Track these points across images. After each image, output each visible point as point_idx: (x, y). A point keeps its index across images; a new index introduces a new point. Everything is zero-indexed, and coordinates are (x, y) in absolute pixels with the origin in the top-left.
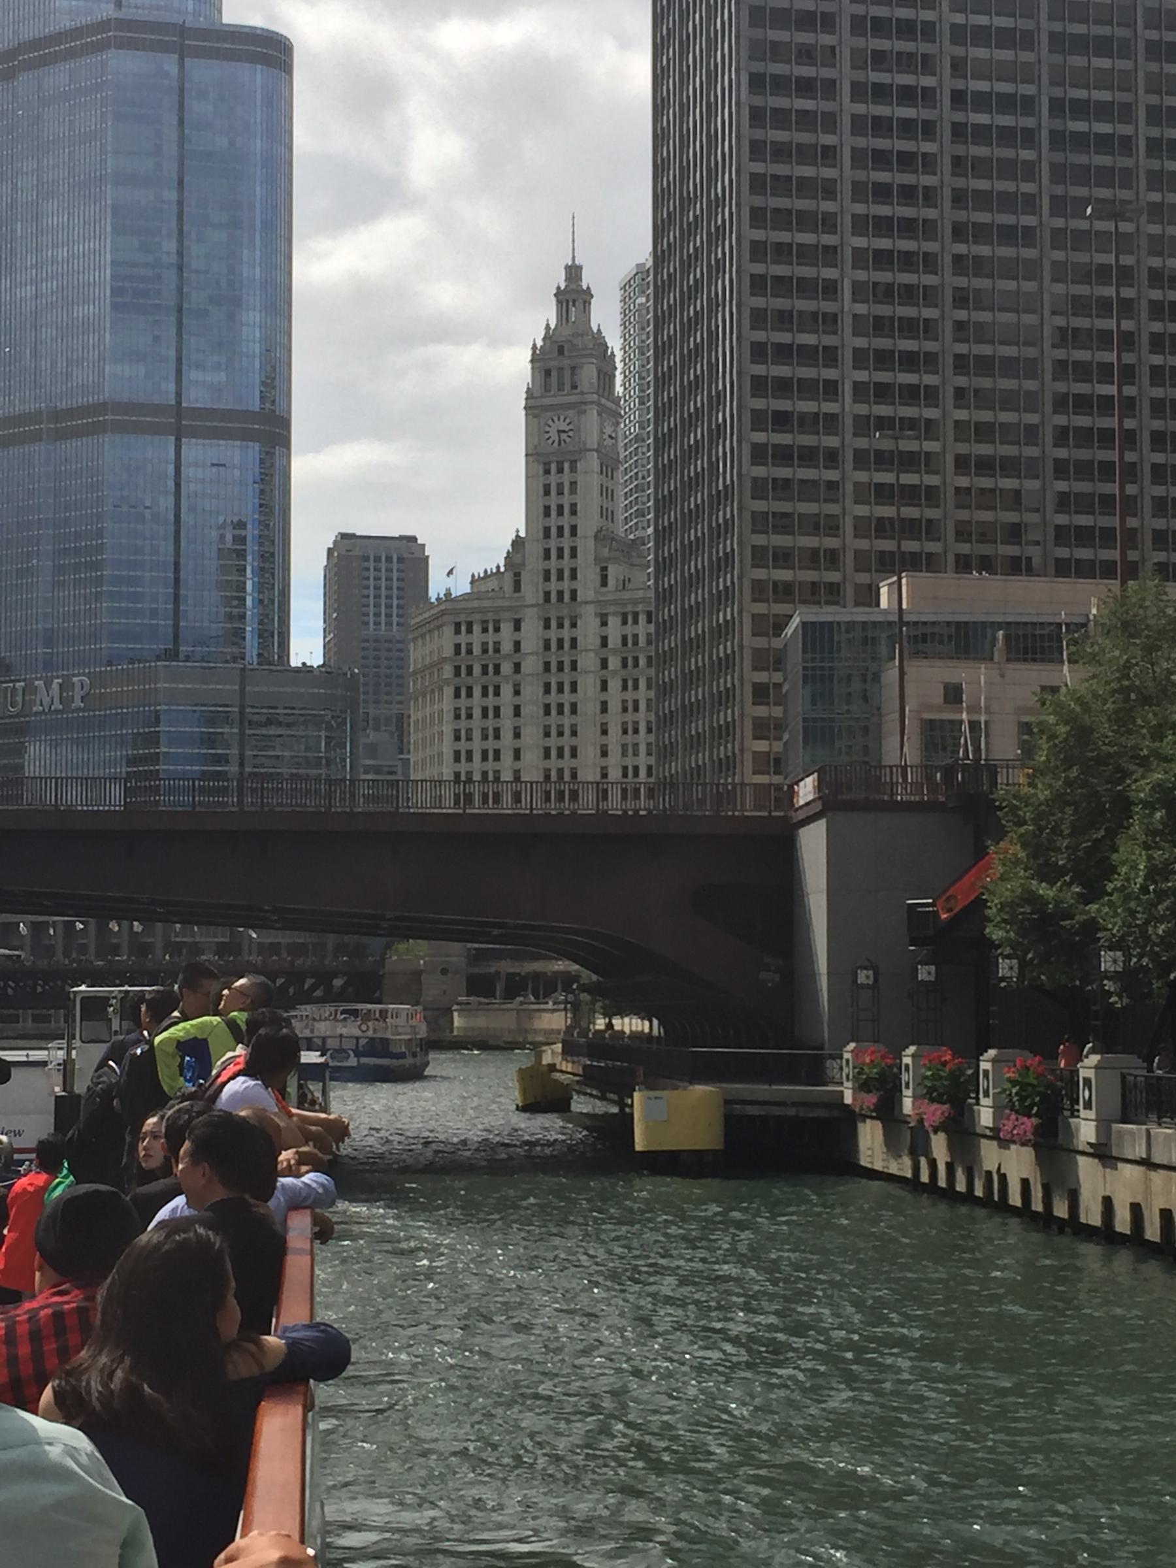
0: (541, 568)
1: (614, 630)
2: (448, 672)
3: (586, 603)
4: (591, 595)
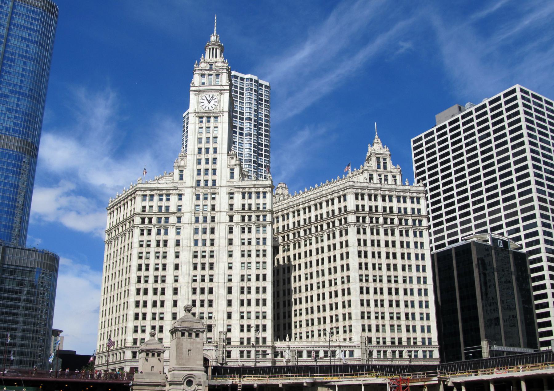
0: (195, 168)
1: (238, 202)
2: (137, 220)
3: (221, 186)
4: (224, 183)
